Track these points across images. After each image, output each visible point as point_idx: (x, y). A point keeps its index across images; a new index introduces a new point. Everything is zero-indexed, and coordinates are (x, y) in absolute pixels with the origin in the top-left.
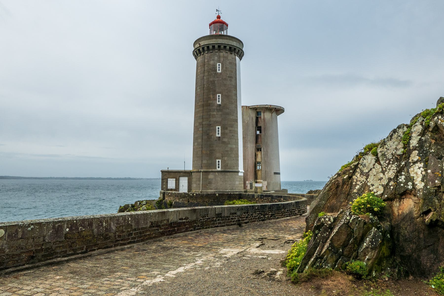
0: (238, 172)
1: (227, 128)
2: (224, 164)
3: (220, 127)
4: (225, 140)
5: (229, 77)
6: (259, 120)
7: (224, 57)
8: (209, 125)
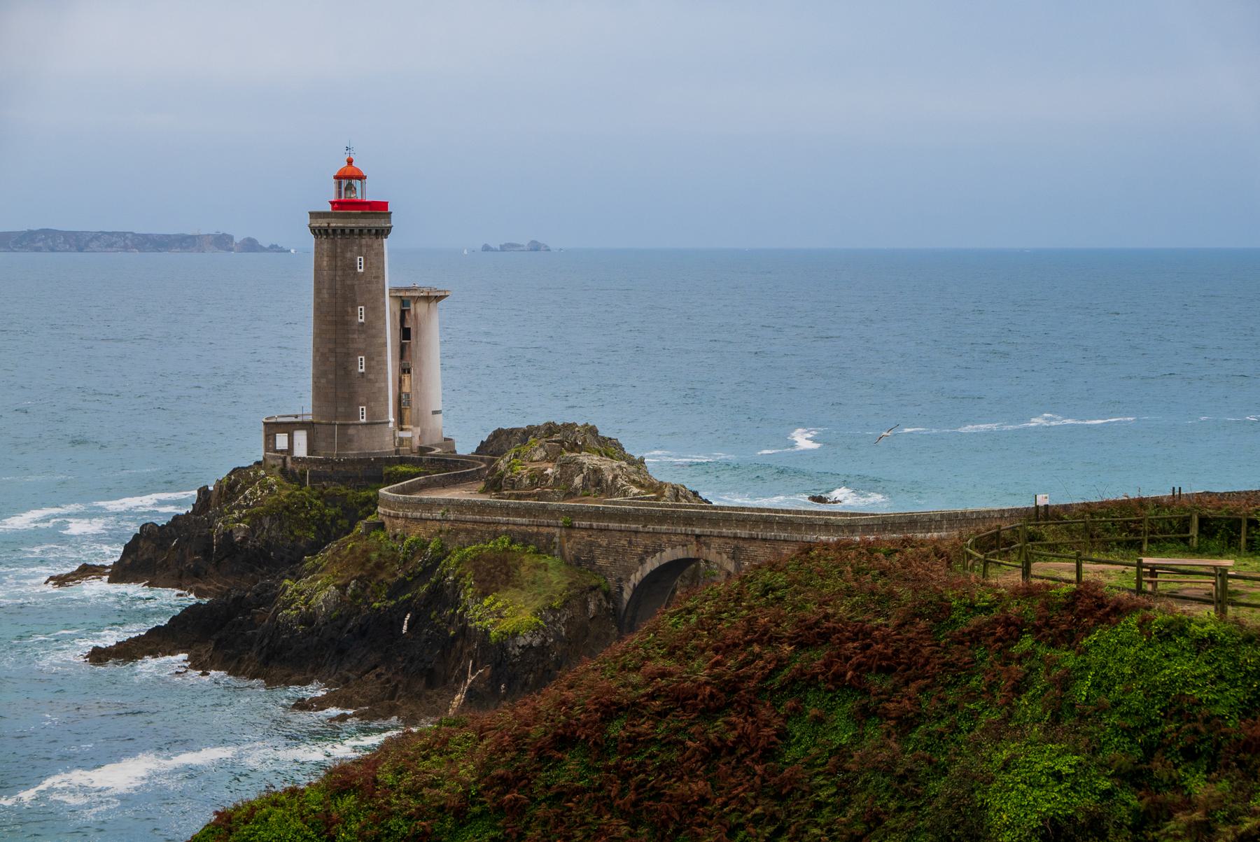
0: (388, 422)
1: (373, 359)
2: (371, 414)
3: (363, 357)
4: (371, 376)
5: (375, 278)
6: (407, 317)
7: (367, 246)
8: (348, 355)
